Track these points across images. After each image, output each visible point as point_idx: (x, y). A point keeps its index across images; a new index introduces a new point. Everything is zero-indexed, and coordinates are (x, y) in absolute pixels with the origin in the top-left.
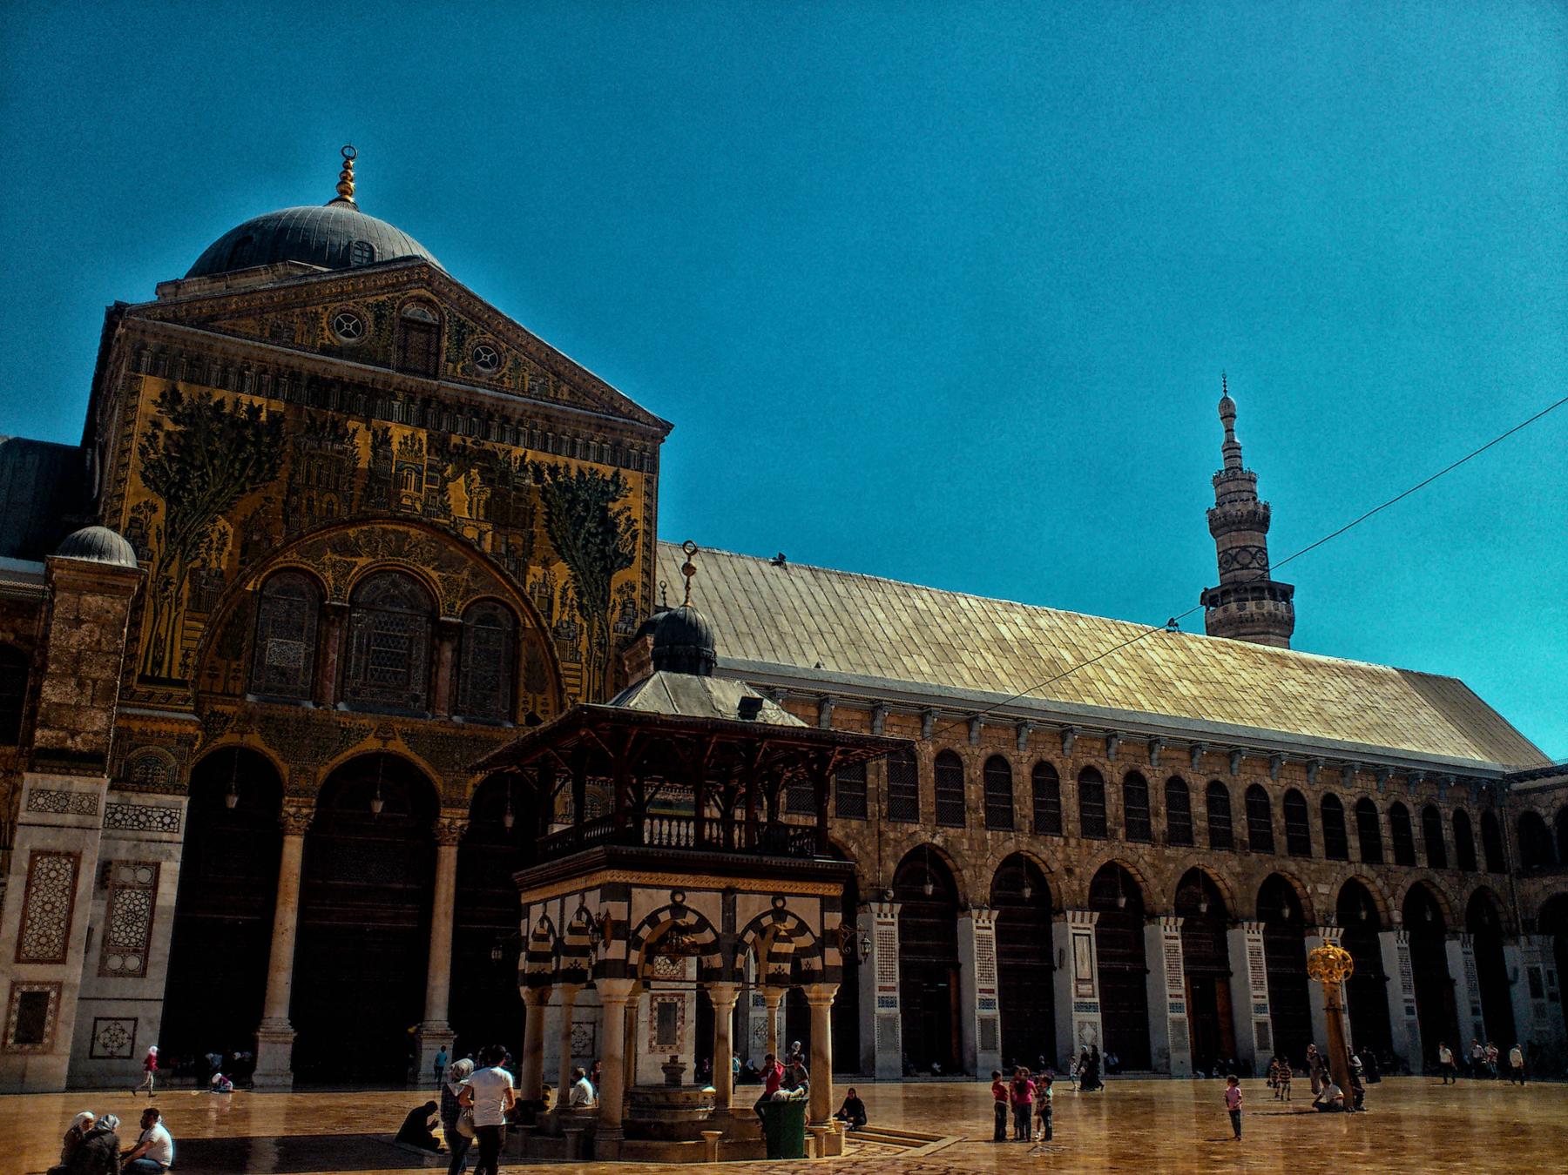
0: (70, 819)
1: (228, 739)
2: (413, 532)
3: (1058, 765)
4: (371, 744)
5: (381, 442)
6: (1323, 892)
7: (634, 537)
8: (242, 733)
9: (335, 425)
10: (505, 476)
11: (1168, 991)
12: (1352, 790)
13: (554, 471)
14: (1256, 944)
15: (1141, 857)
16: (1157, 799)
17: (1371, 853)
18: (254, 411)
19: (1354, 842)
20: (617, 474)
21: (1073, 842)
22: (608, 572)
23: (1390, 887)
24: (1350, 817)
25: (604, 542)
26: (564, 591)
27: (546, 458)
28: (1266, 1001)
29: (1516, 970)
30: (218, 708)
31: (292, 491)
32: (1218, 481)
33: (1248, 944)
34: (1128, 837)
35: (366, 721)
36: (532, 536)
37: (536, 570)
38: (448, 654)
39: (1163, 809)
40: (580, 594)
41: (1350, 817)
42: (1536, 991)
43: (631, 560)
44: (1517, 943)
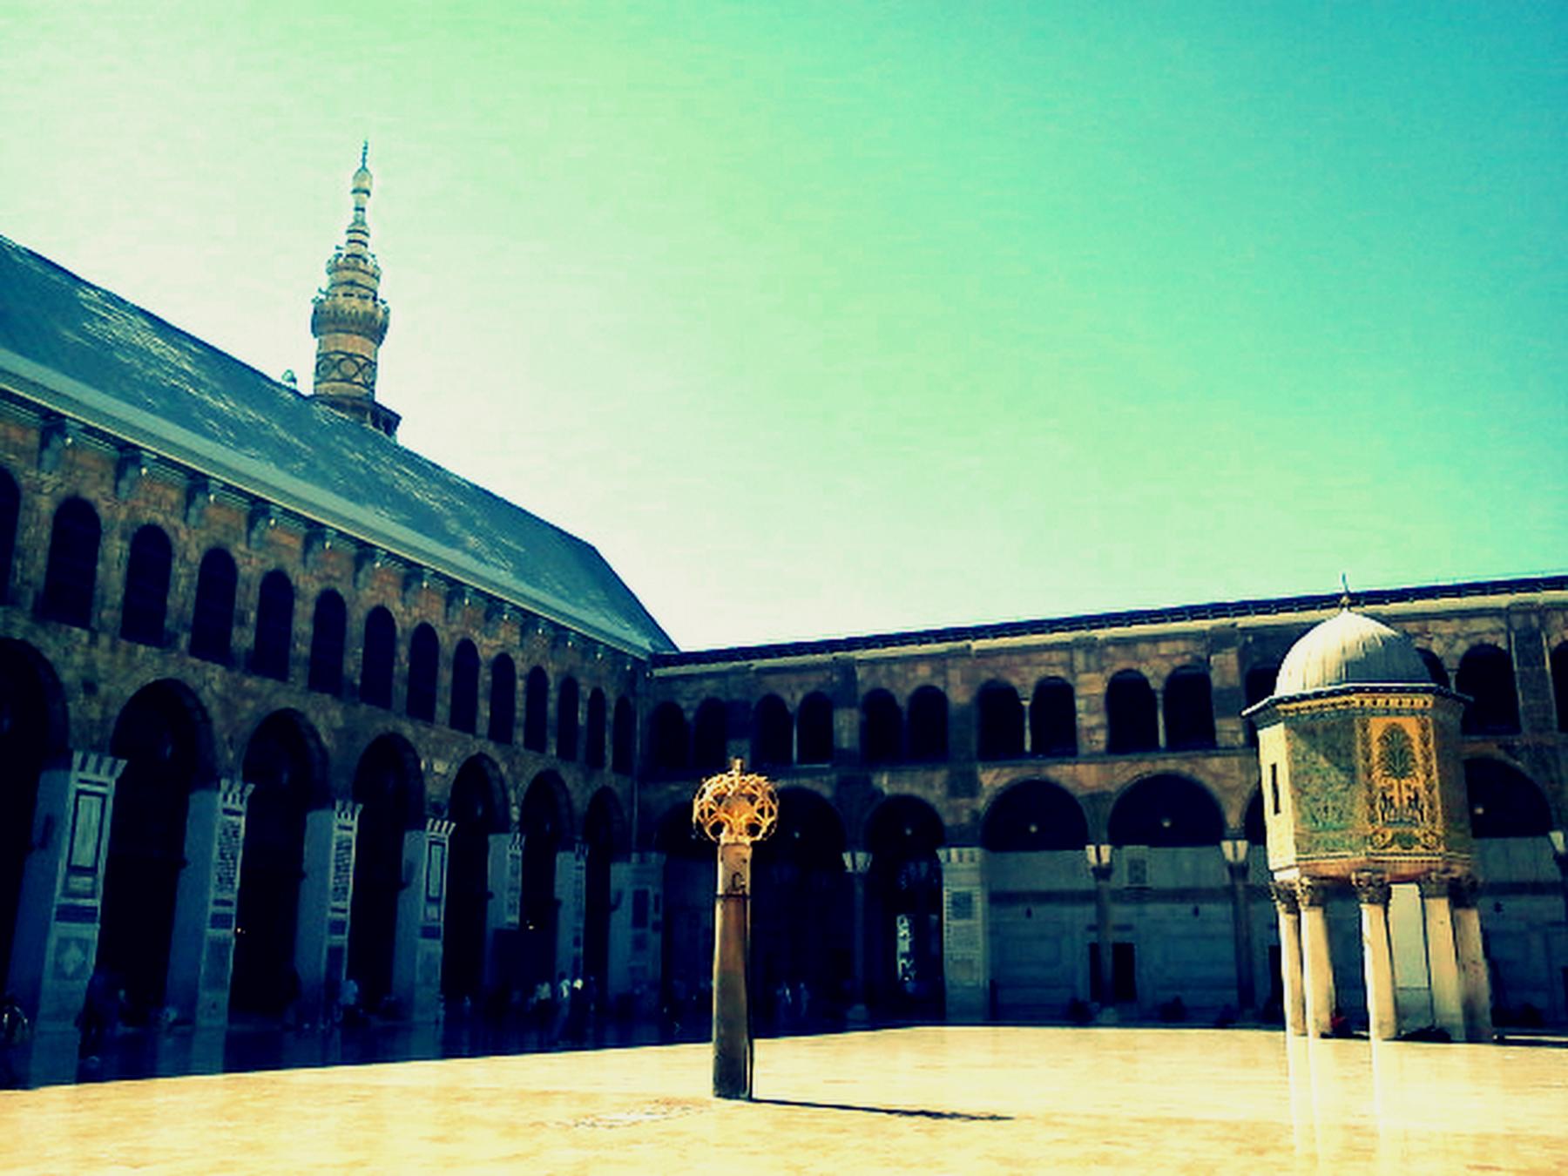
3: (103, 509)
6: (440, 769)
11: (213, 894)
12: (494, 642)
14: (346, 833)
15: (211, 680)
16: (248, 599)
17: (500, 732)
19: (484, 710)
21: (104, 640)
23: (518, 769)
24: (485, 677)
28: (346, 917)
29: (620, 895)
32: (334, 268)
33: (337, 832)
34: (194, 650)
39: (253, 615)
41: (485, 677)
42: (639, 919)
44: (628, 860)
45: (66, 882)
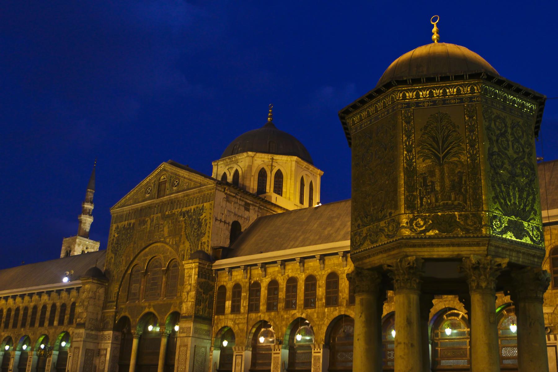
0: (79, 339)
1: (123, 314)
2: (159, 244)
4: (147, 310)
5: (152, 221)
7: (206, 225)
8: (125, 312)
9: (144, 220)
13: (188, 212)
18: (130, 224)
20: (203, 206)
22: (198, 240)
25: (198, 230)
26: (187, 250)
30: (123, 306)
31: (135, 243)
35: (147, 304)
36: (181, 235)
37: (182, 246)
38: (164, 279)
40: (191, 250)
43: (205, 234)
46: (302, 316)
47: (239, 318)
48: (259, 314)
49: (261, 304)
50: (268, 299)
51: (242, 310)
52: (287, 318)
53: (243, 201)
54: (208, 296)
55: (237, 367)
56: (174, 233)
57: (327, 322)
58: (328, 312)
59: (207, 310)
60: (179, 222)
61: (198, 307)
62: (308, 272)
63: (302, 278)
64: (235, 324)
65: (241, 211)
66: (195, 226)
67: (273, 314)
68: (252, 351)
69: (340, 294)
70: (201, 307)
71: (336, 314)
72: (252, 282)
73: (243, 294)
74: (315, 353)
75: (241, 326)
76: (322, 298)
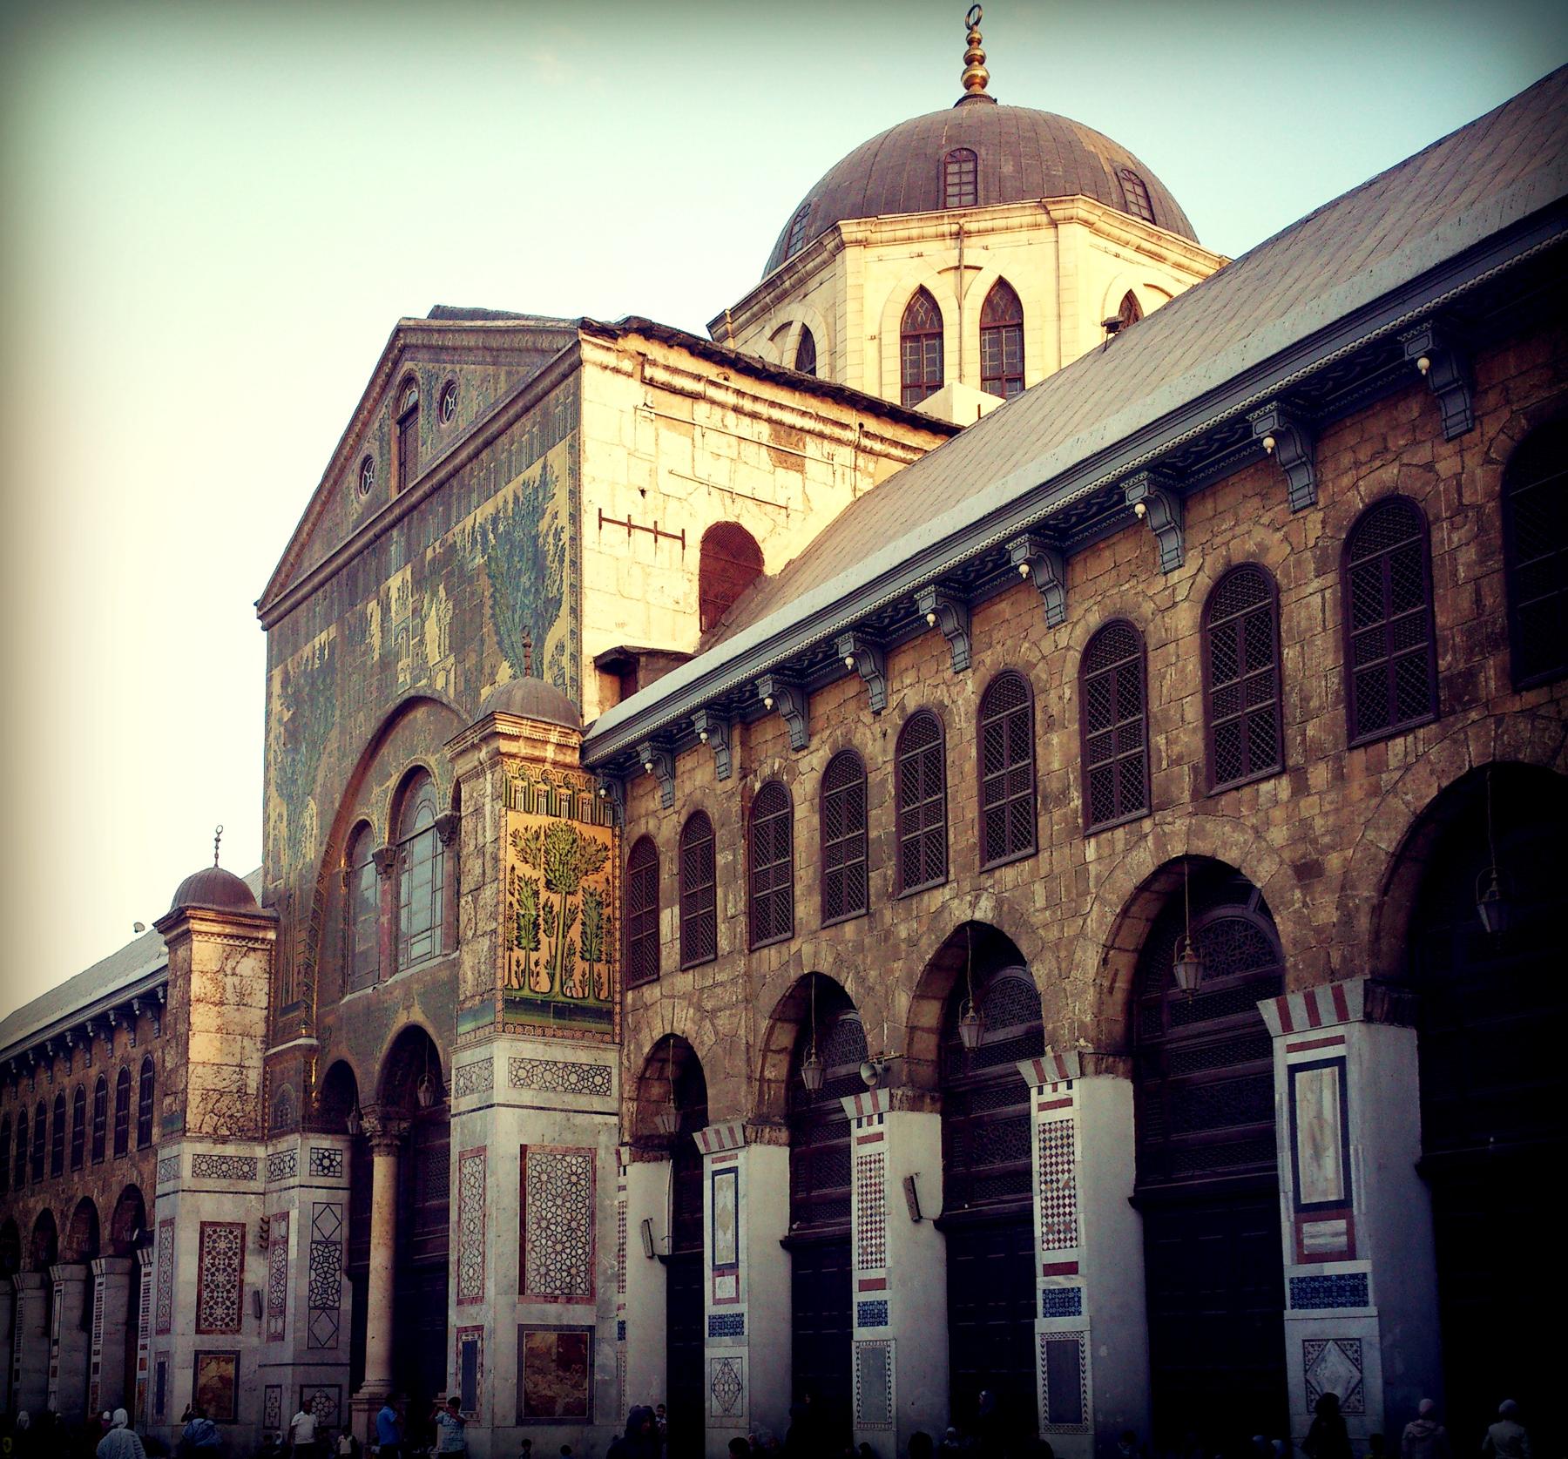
4: (401, 1020)
5: (386, 610)
10: (461, 567)
13: (495, 520)
21: (1319, 775)
22: (541, 640)
27: (488, 509)
43: (558, 603)
45: (1298, 1231)
46: (978, 916)
47: (715, 985)
48: (794, 947)
49: (799, 890)
50: (829, 855)
51: (723, 944)
52: (913, 942)
53: (754, 416)
54: (578, 899)
55: (719, 1234)
56: (460, 639)
57: (1099, 918)
58: (1099, 859)
59: (580, 966)
60: (470, 581)
61: (519, 954)
62: (991, 660)
63: (961, 699)
64: (706, 1015)
65: (758, 473)
66: (524, 579)
67: (849, 930)
68: (791, 1144)
69: (1159, 740)
70: (543, 955)
71: (1144, 861)
72: (758, 786)
73: (723, 859)
74: (1043, 1107)
75: (723, 1020)
76: (1065, 792)
